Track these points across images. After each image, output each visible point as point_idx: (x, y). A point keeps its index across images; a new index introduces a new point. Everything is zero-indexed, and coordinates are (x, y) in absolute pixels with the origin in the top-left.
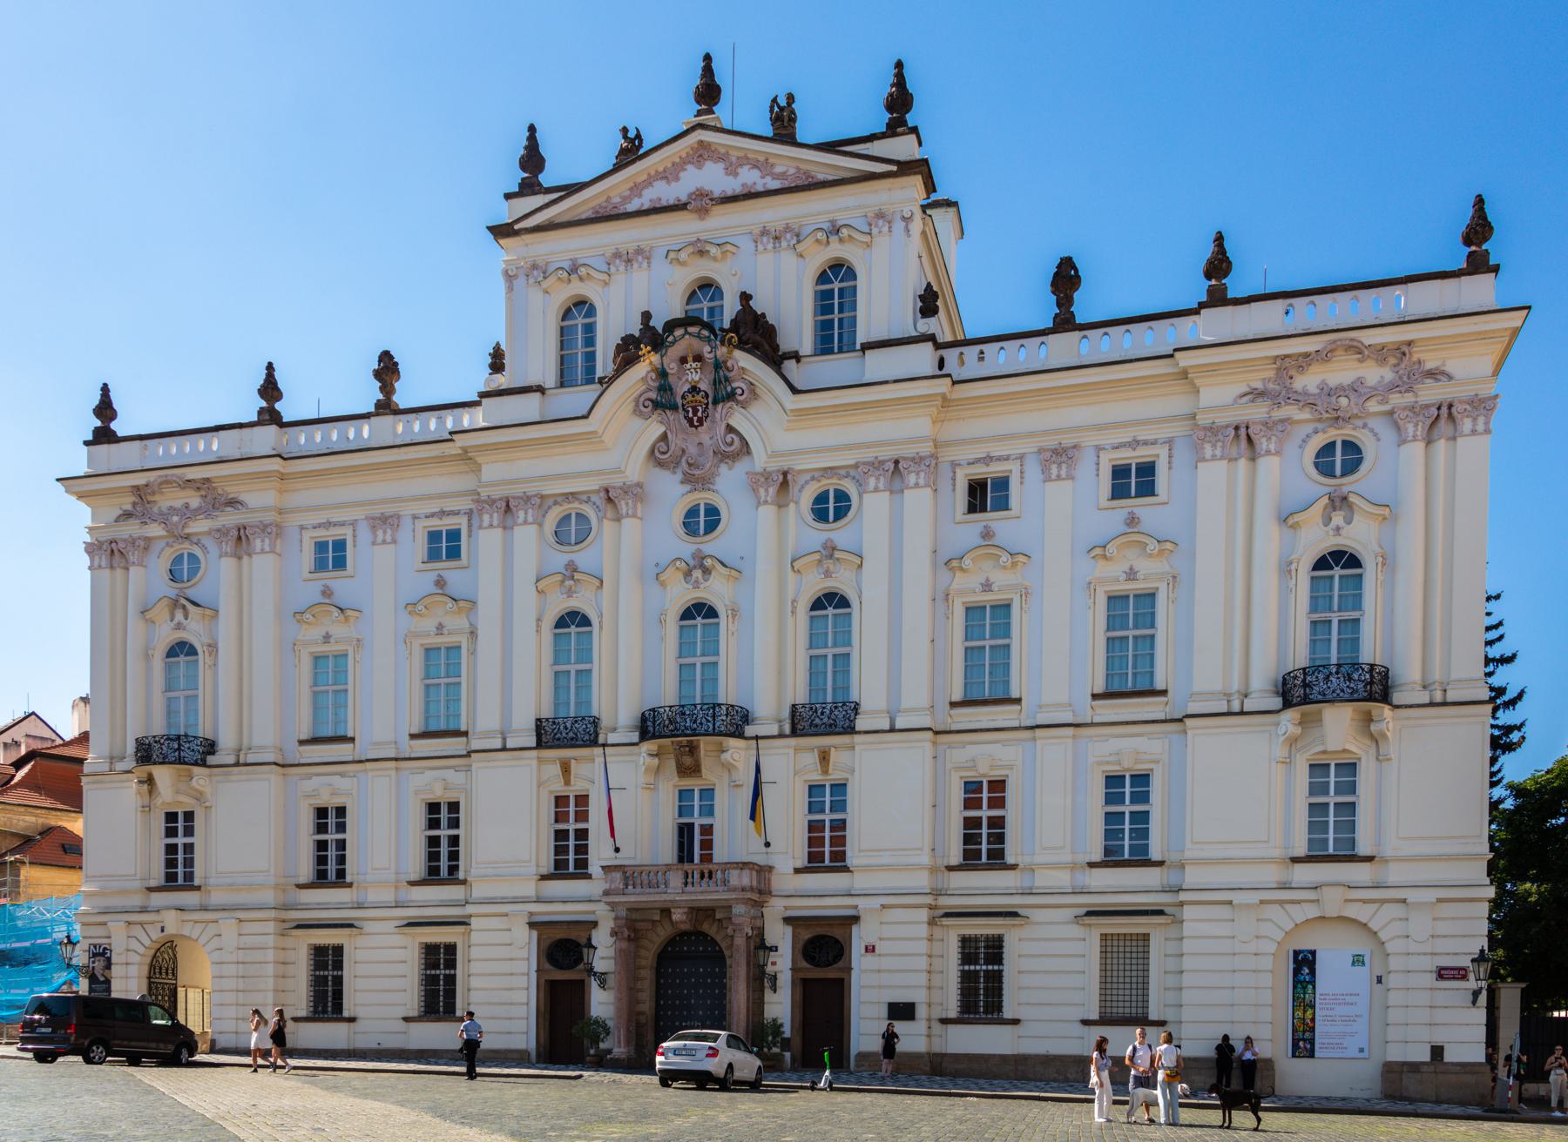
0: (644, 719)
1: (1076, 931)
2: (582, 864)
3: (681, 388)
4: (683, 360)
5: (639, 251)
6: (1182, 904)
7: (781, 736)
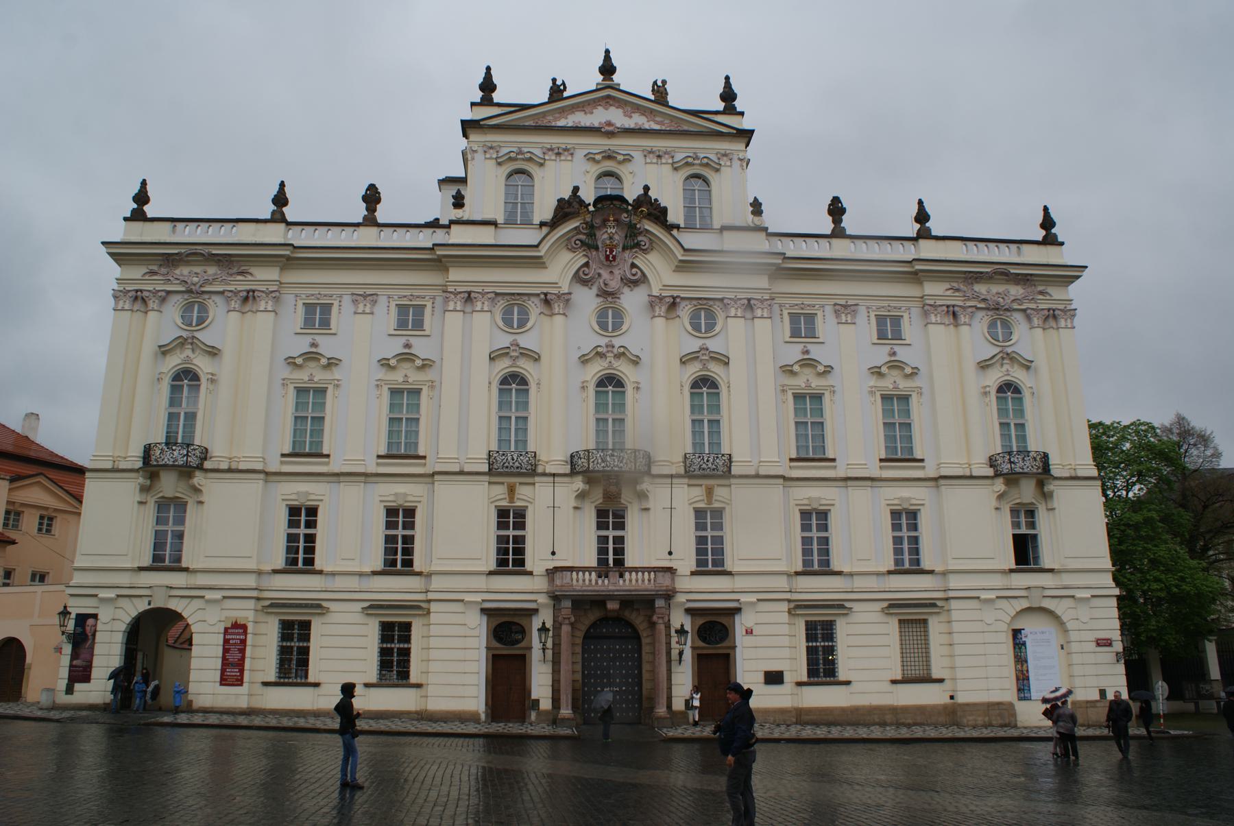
0: (572, 456)
1: (880, 617)
2: (521, 563)
3: (602, 236)
4: (605, 221)
5: (566, 150)
6: (947, 599)
7: (679, 476)
